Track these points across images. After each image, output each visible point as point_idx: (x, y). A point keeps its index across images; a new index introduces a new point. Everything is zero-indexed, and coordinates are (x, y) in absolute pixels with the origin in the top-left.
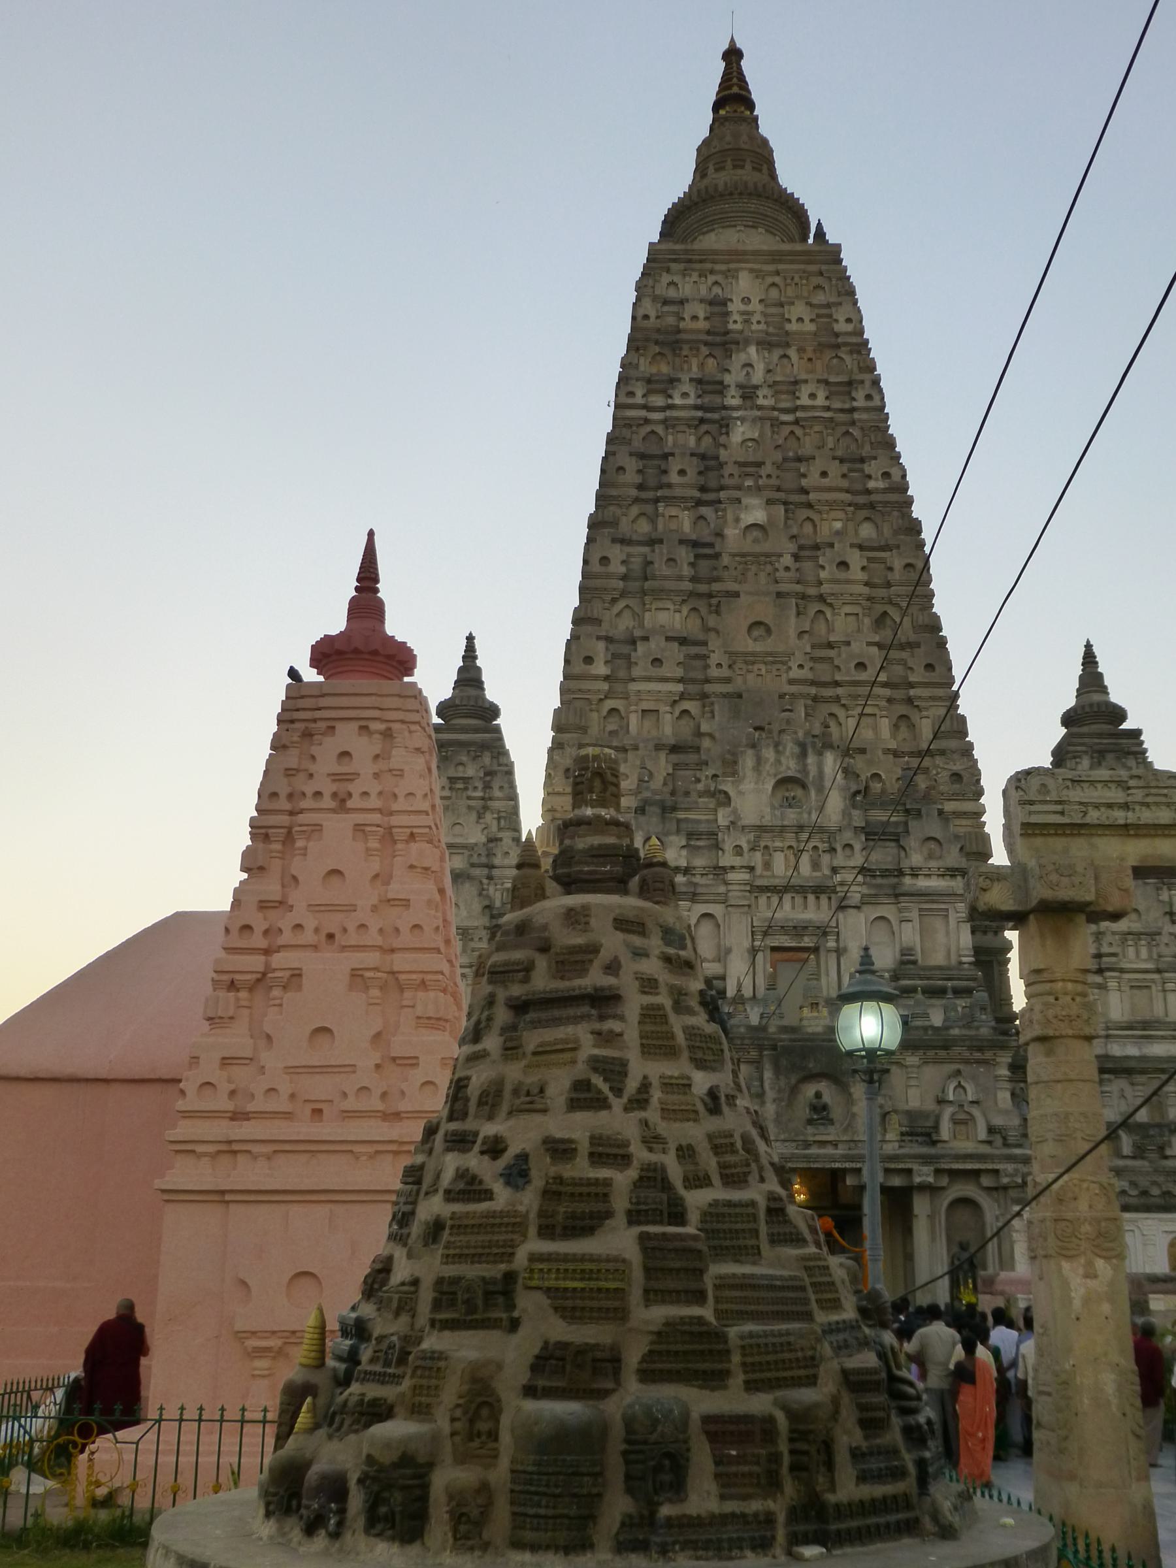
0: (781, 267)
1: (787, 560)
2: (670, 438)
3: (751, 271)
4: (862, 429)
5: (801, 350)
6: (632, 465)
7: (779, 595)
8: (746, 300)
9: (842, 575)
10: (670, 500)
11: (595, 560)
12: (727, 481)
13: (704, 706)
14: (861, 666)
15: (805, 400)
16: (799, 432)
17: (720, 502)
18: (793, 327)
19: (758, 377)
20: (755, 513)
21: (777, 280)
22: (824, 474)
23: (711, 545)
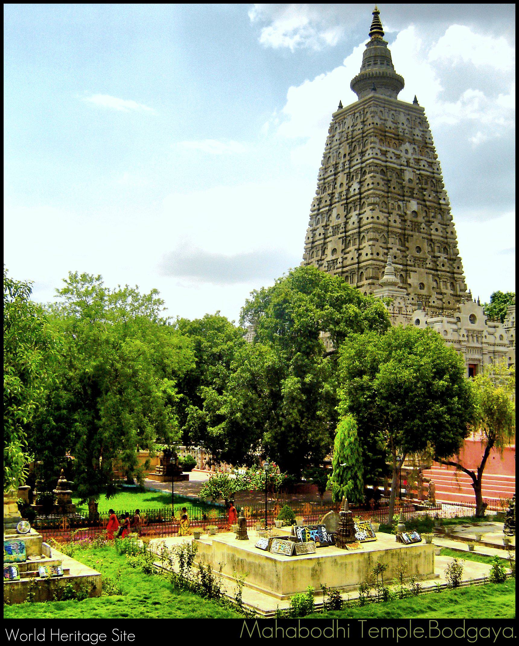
0: (410, 113)
1: (423, 225)
2: (388, 173)
3: (404, 113)
4: (436, 180)
5: (418, 147)
6: (382, 183)
7: (423, 238)
8: (403, 124)
9: (436, 233)
10: (393, 198)
11: (375, 217)
12: (406, 194)
13: (406, 274)
14: (443, 265)
15: (422, 167)
16: (420, 178)
17: (404, 200)
18: (416, 138)
19: (409, 156)
20: (414, 205)
21: (409, 117)
22: (429, 196)
23: (403, 216)
